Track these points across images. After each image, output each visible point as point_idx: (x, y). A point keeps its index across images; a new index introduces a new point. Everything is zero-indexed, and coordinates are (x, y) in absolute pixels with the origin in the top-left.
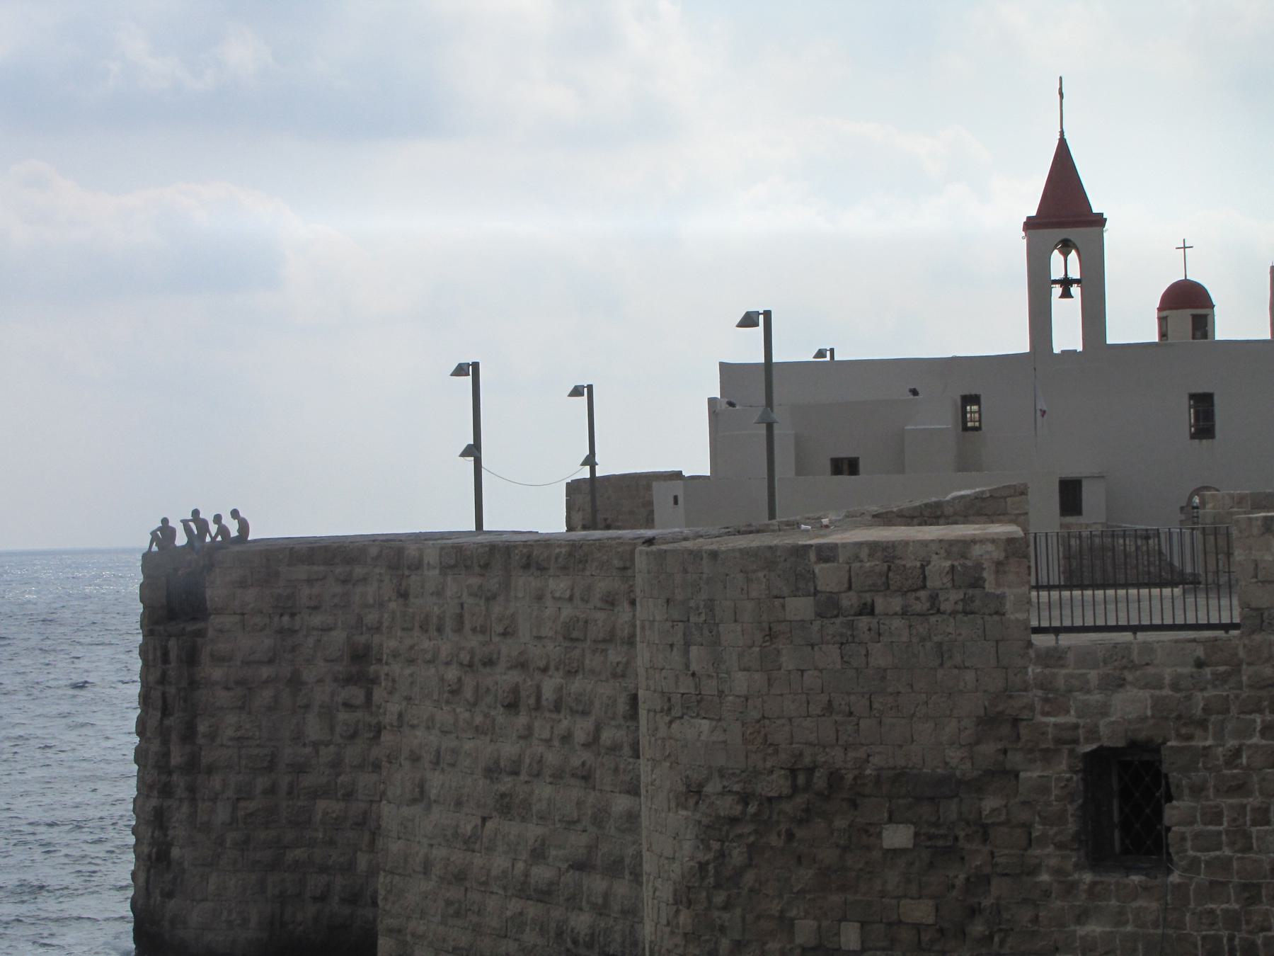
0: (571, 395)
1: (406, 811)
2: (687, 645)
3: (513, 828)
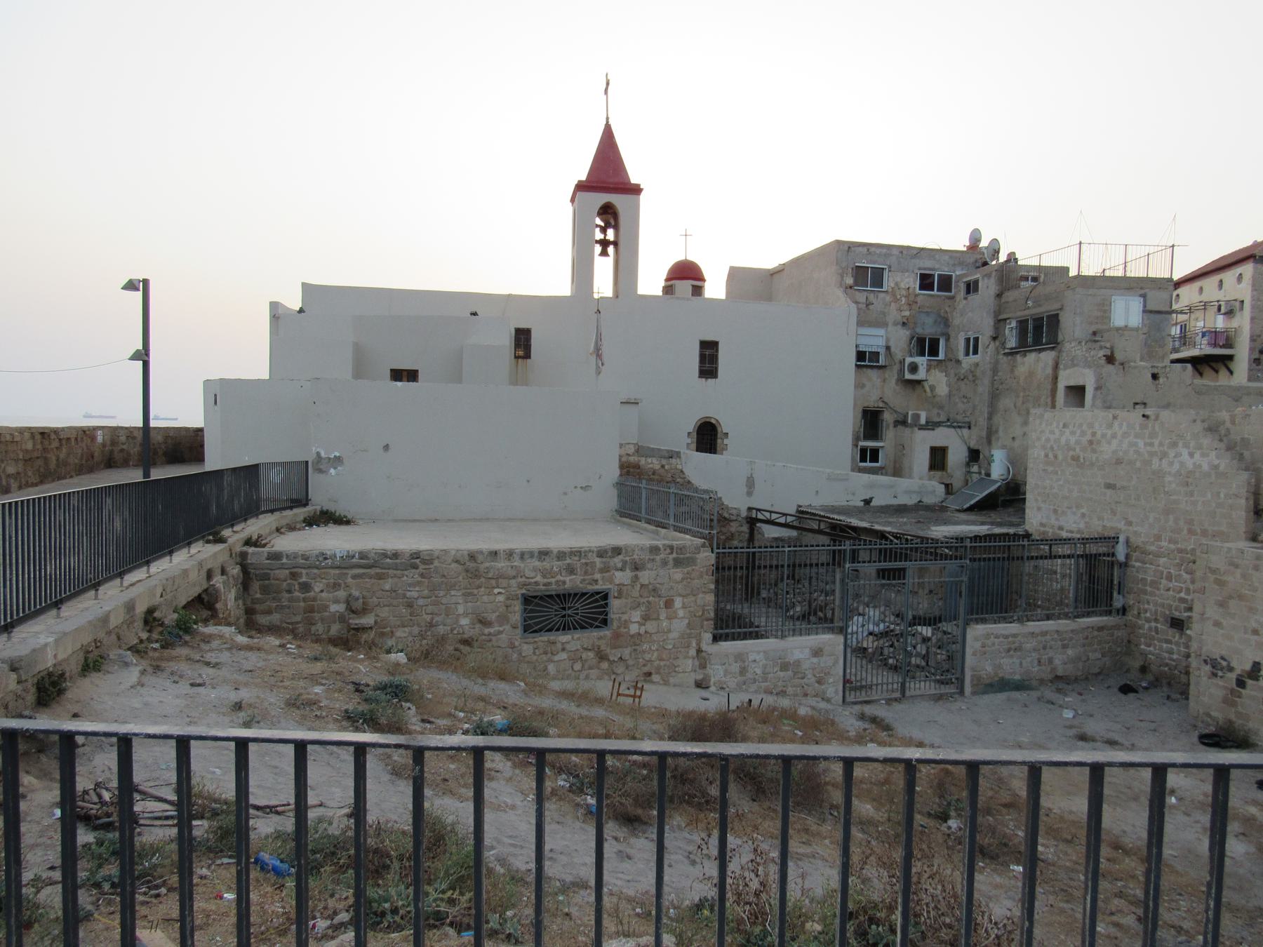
0: (125, 288)
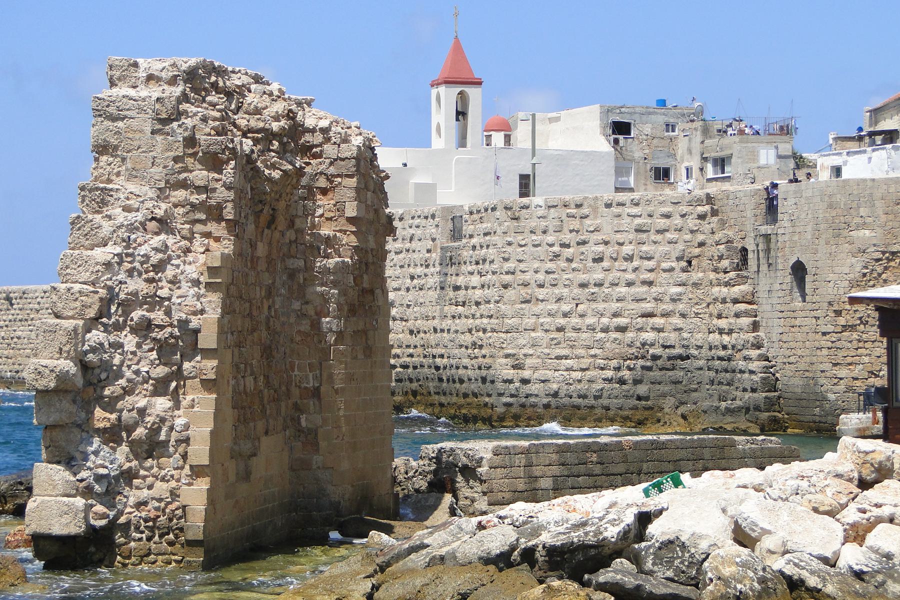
1: (519, 306)
3: (601, 306)
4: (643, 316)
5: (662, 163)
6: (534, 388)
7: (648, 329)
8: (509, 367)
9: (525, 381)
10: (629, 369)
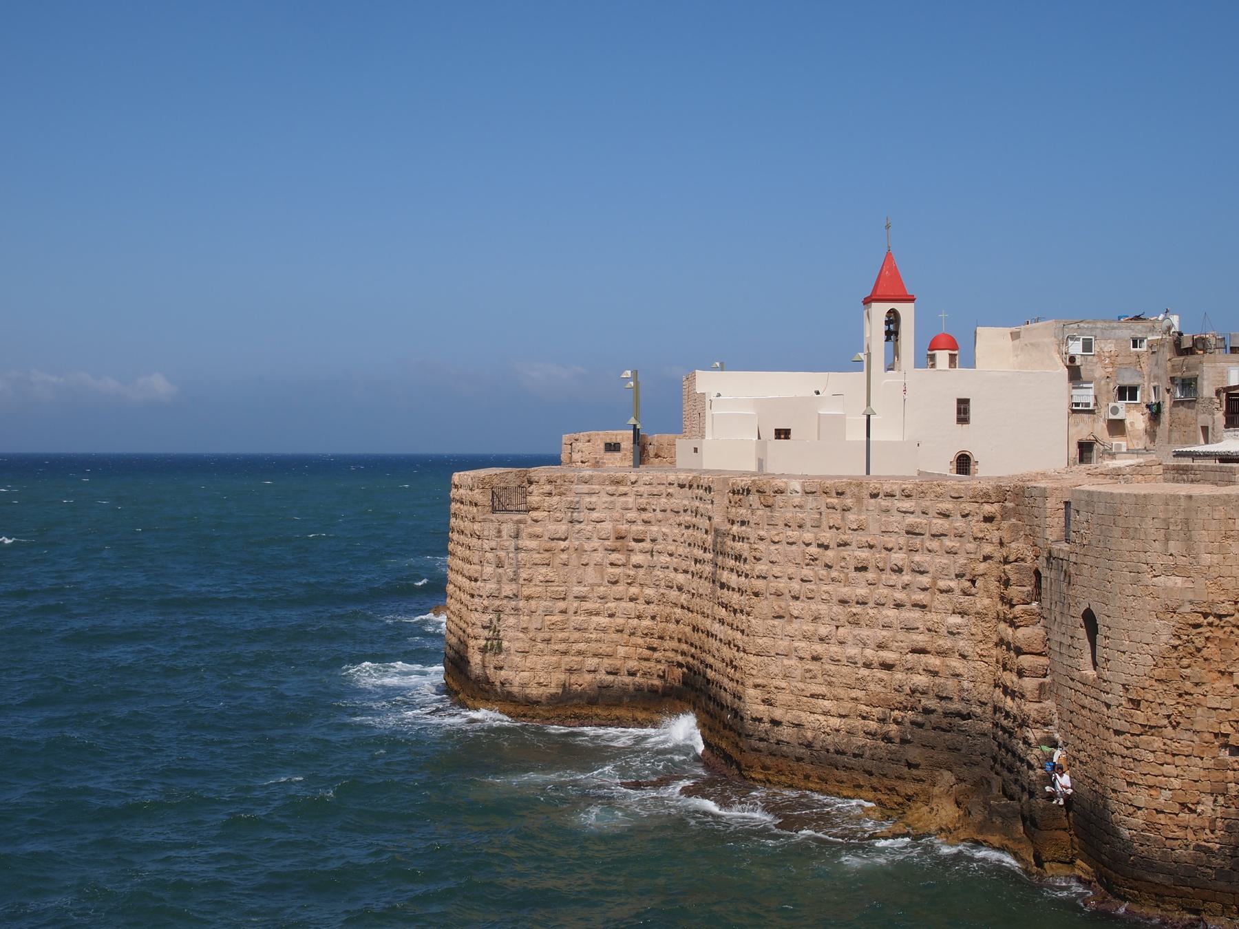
1: (771, 622)
2: (1167, 540)
3: (864, 632)
4: (914, 651)
5: (1128, 381)
6: (786, 733)
7: (921, 671)
8: (759, 701)
9: (775, 723)
10: (896, 721)
